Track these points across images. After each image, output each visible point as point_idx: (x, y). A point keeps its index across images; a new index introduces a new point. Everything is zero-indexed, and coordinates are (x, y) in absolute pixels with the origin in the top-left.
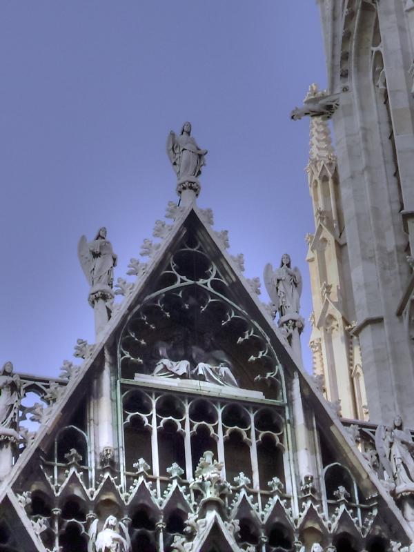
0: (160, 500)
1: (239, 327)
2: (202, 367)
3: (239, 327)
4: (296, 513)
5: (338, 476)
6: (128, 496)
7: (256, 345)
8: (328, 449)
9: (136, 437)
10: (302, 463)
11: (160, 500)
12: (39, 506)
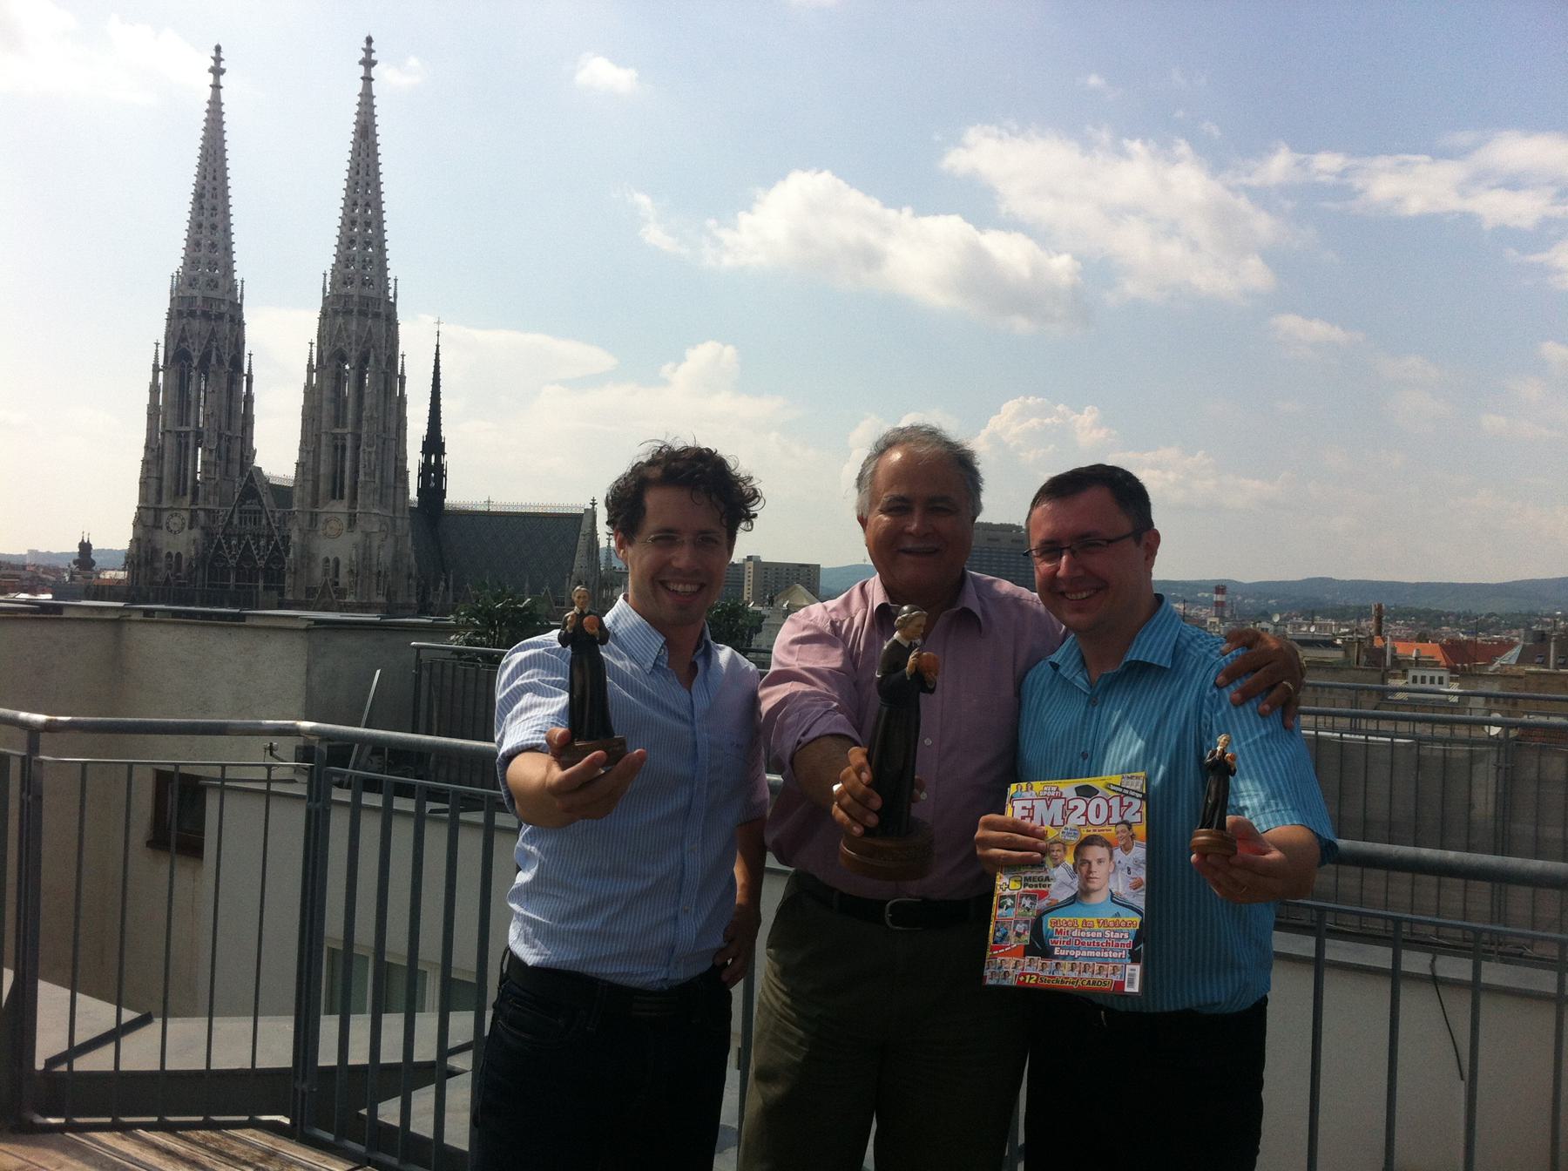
10: (264, 522)
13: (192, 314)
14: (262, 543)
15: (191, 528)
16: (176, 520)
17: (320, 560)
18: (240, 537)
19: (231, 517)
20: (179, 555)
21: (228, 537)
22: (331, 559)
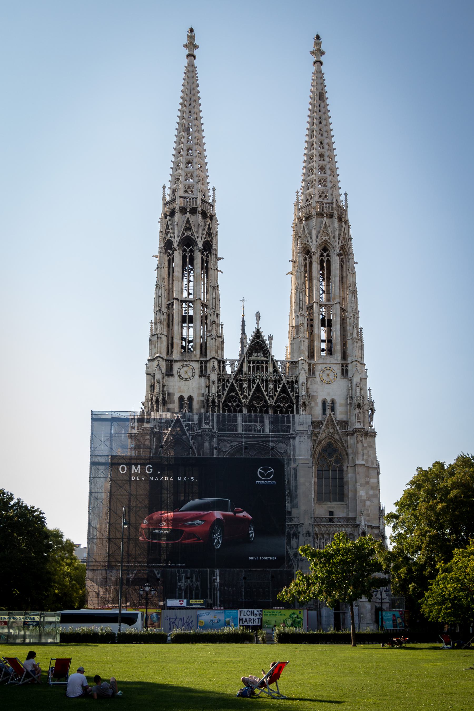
0: (252, 378)
1: (264, 347)
2: (259, 354)
3: (264, 347)
4: (269, 378)
5: (276, 371)
6: (247, 378)
7: (266, 350)
8: (274, 366)
9: (249, 367)
10: (271, 369)
11: (252, 378)
12: (237, 380)
13: (194, 211)
14: (271, 386)
15: (200, 376)
16: (185, 368)
17: (319, 401)
18: (250, 382)
20: (190, 398)
21: (239, 382)
22: (329, 400)
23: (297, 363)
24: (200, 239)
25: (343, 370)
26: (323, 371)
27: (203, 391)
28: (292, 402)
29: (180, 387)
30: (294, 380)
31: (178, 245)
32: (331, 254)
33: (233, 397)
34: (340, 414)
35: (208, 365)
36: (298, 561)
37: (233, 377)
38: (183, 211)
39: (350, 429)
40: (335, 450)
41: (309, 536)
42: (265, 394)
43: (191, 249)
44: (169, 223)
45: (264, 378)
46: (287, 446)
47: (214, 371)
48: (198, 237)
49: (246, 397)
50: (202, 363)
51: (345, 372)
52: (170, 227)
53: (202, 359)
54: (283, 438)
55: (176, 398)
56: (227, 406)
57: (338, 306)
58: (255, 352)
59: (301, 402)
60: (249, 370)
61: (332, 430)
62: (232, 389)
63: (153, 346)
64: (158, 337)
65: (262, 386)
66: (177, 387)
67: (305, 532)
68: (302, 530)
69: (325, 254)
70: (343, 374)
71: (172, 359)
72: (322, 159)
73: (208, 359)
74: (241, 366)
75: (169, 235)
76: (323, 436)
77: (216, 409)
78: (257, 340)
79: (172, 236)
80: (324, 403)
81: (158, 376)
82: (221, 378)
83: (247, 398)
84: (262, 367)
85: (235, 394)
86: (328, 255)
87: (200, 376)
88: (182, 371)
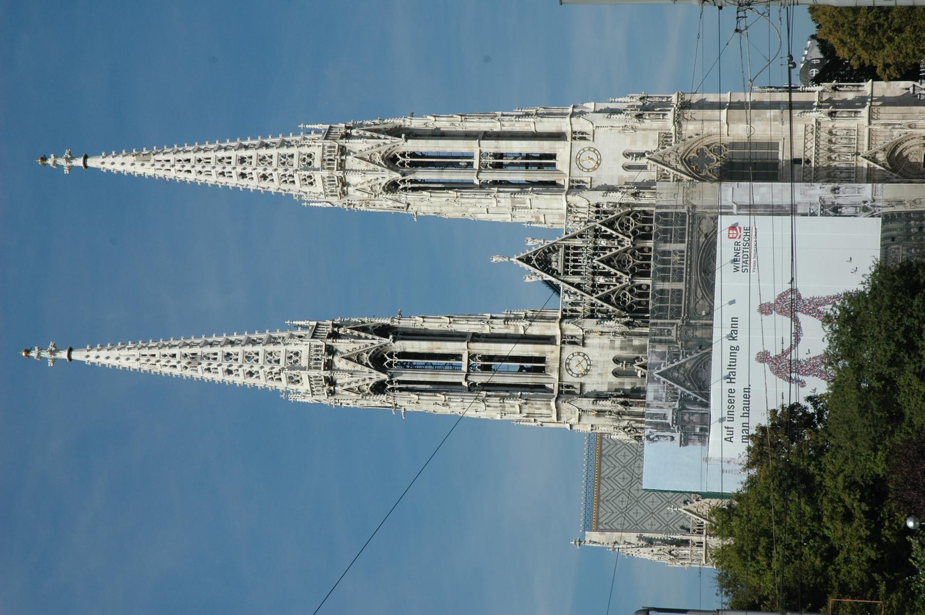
2: (553, 259)
3: (544, 252)
6: (591, 276)
7: (549, 249)
8: (574, 237)
9: (574, 273)
10: (578, 242)
12: (593, 291)
14: (603, 243)
15: (584, 345)
16: (573, 364)
19: (572, 284)
20: (616, 360)
21: (595, 287)
23: (569, 206)
24: (374, 341)
25: (581, 138)
26: (581, 168)
27: (605, 340)
28: (629, 214)
29: (600, 374)
30: (595, 209)
31: (385, 372)
32: (401, 150)
33: (618, 299)
34: (650, 144)
35: (568, 333)
36: (874, 206)
37: (587, 297)
38: (329, 366)
39: (672, 131)
40: (701, 152)
41: (838, 188)
42: (614, 251)
43: (388, 355)
44: (346, 387)
45: (592, 251)
46: (705, 218)
47: (579, 323)
48: (372, 344)
49: (619, 280)
50: (563, 343)
51: (581, 136)
52: (353, 385)
53: (559, 342)
54: (693, 223)
55: (616, 380)
56: (631, 307)
57: (482, 142)
58: (550, 264)
59: (632, 200)
60: (578, 273)
61: (673, 156)
62: (606, 299)
63: (537, 412)
64: (526, 404)
65: (602, 256)
66: (600, 380)
67: (832, 196)
68: (829, 197)
69: (402, 159)
70: (585, 139)
71: (556, 385)
72: (248, 160)
73: (558, 333)
74: (572, 284)
75: (365, 387)
76: (680, 167)
77: (639, 321)
78: (534, 262)
79: (368, 381)
80: (628, 168)
81: (586, 404)
82: (589, 313)
83: (621, 277)
84: (574, 255)
85: (613, 294)
86: (403, 155)
87: (584, 345)
88: (577, 370)
